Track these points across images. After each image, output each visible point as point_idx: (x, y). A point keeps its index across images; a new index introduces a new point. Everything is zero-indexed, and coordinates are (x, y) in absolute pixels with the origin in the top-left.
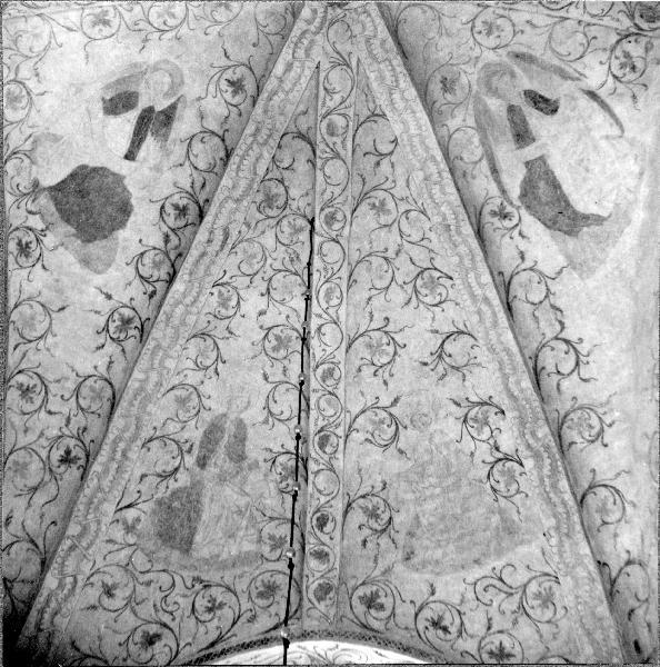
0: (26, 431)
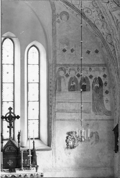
0: (93, 17)
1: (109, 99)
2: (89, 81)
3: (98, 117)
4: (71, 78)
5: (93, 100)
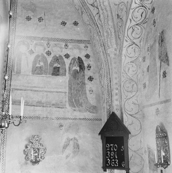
1: (94, 89)
2: (64, 62)
3: (78, 114)
4: (38, 56)
5: (70, 88)
